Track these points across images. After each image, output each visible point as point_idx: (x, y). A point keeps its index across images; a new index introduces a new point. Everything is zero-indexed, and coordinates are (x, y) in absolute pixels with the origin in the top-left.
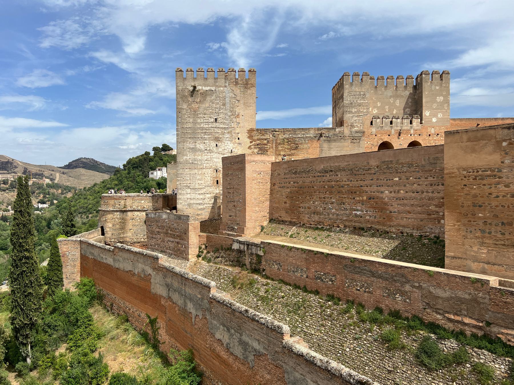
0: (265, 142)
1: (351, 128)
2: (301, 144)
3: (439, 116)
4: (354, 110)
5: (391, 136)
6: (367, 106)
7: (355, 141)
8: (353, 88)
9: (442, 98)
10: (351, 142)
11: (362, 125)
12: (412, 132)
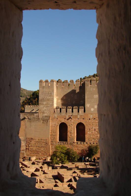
1: (43, 114)
3: (95, 107)
4: (45, 103)
11: (49, 112)
12: (79, 117)
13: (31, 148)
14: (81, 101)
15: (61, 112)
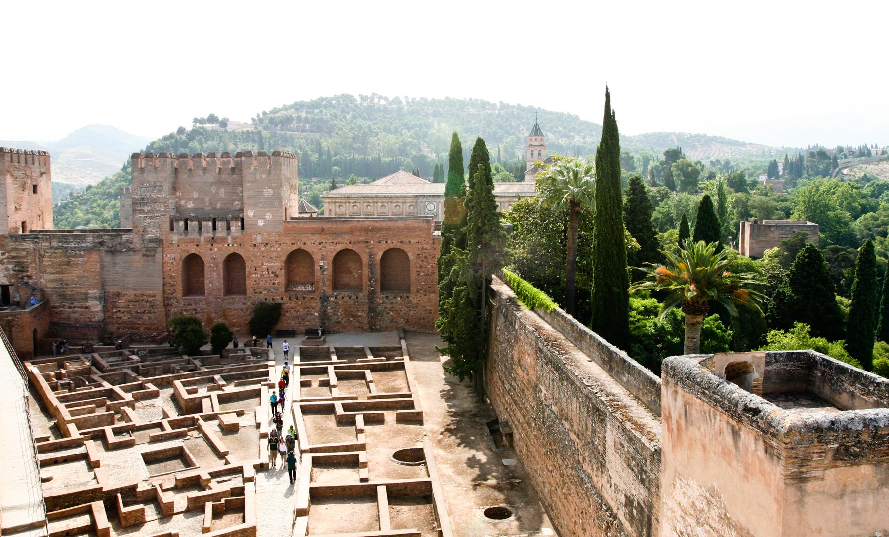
0: (24, 253)
2: (75, 257)
3: (267, 217)
4: (146, 209)
8: (145, 175)
9: (270, 191)
10: (144, 255)
13: (119, 315)
14: (236, 202)
15: (186, 228)
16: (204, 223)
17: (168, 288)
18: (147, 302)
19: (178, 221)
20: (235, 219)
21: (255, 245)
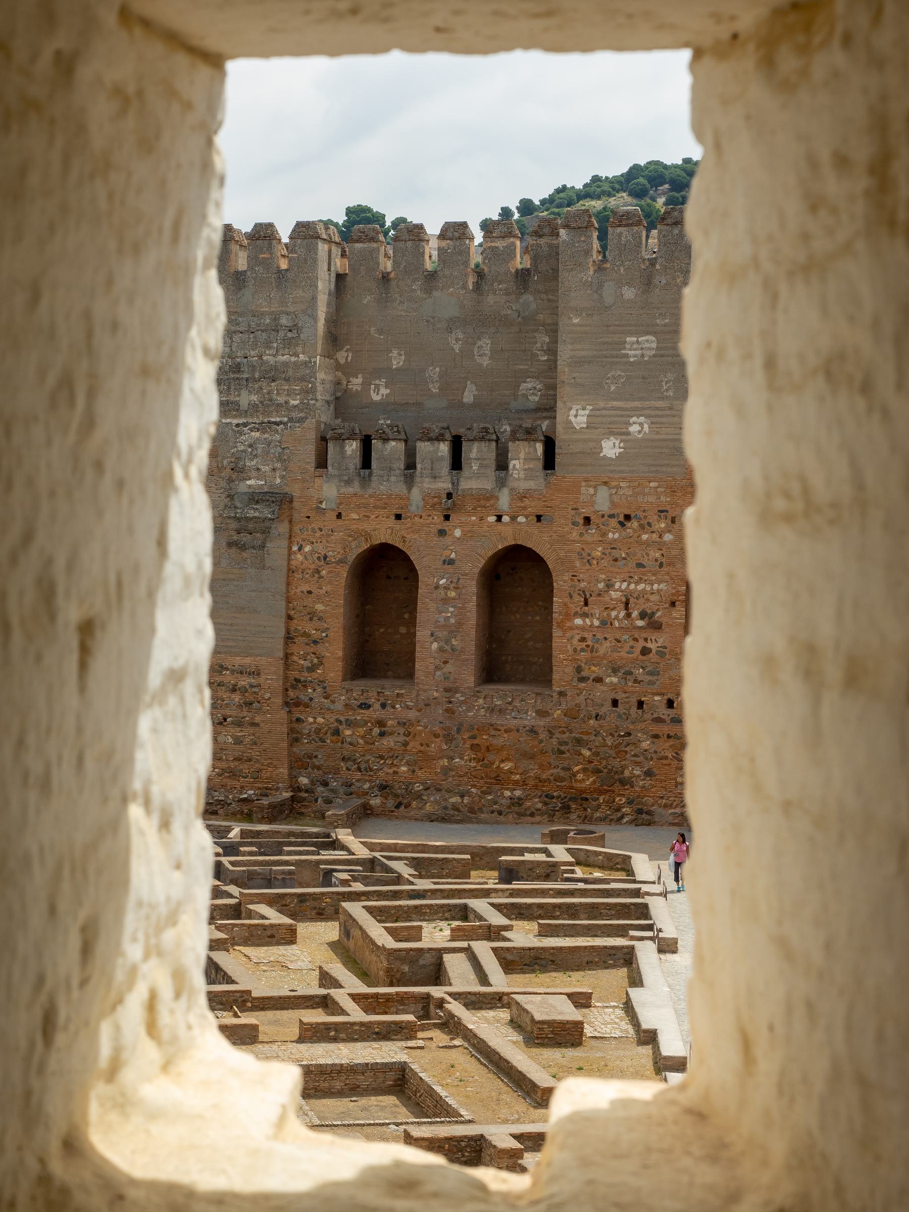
1: (230, 480)
3: (634, 429)
5: (405, 522)
6: (303, 379)
7: (245, 538)
9: (649, 342)
11: (278, 465)
12: (504, 501)
15: (366, 462)
16: (423, 448)
17: (299, 649)
18: (234, 690)
19: (340, 439)
20: (529, 434)
21: (587, 520)
